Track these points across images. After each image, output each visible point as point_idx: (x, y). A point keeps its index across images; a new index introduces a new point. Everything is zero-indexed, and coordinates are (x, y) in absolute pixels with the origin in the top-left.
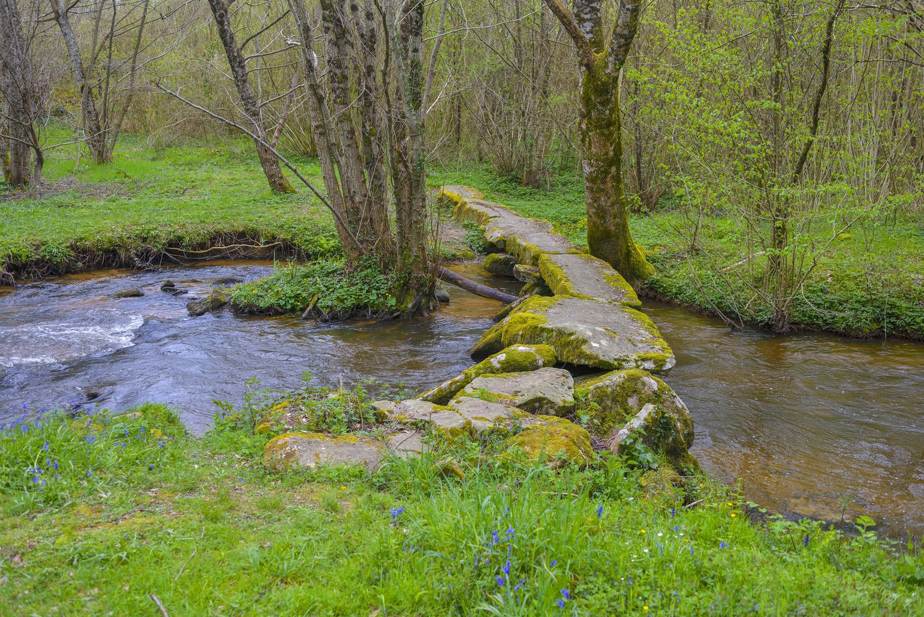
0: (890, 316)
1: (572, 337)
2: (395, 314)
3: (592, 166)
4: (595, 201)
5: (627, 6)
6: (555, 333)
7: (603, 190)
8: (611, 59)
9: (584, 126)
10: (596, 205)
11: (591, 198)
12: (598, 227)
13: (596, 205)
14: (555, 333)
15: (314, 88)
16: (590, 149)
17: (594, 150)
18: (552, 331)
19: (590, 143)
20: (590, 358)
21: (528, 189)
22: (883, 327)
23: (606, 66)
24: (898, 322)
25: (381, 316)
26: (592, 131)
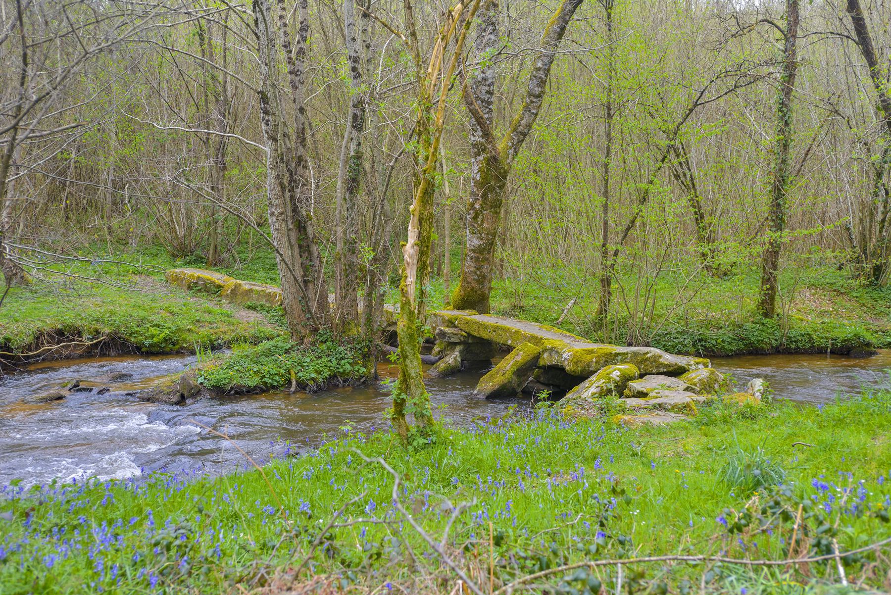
0: (700, 340)
1: (649, 355)
2: (362, 380)
3: (482, 239)
4: (479, 269)
5: (532, 111)
6: (630, 355)
7: (487, 259)
8: (511, 151)
9: (477, 206)
10: (478, 272)
11: (475, 267)
12: (476, 292)
13: (478, 272)
14: (630, 355)
15: (690, 170)
16: (482, 225)
17: (485, 225)
18: (627, 353)
19: (483, 221)
20: (669, 366)
21: (299, 273)
22: (698, 349)
23: (507, 158)
24: (708, 345)
25: (352, 383)
26: (486, 210)
